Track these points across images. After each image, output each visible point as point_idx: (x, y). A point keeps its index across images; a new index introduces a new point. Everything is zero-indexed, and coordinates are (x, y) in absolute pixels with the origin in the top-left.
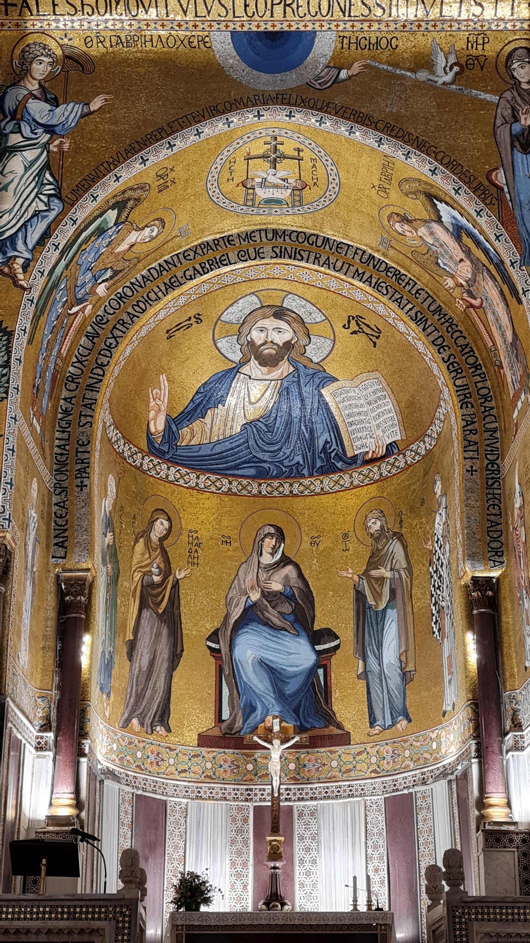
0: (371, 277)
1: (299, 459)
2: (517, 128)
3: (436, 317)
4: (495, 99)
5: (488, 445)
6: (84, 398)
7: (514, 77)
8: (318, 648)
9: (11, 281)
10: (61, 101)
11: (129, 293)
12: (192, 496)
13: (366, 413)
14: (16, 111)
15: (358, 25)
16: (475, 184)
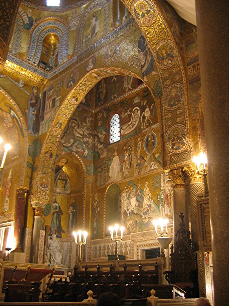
2: (32, 102)
4: (29, 94)
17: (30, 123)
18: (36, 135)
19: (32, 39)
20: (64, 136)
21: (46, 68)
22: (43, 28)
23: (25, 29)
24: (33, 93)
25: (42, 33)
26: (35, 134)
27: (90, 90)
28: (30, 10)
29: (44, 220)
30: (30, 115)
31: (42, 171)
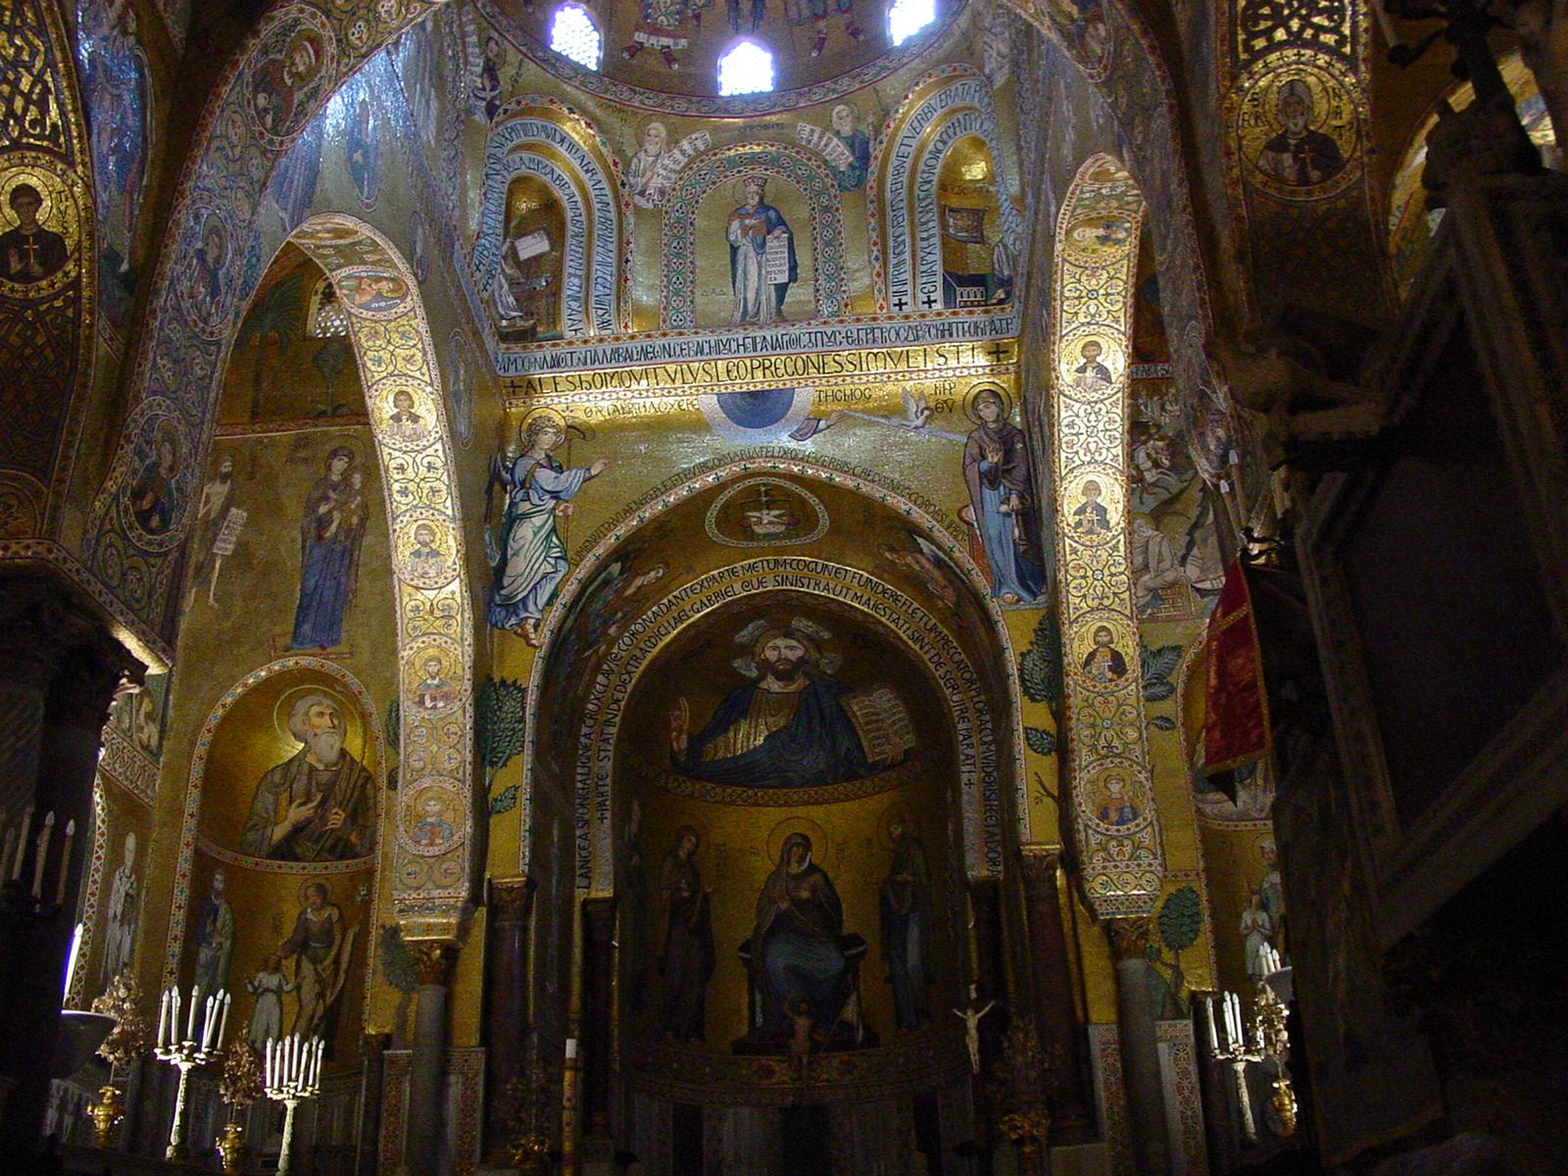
0: (869, 599)
1: (822, 766)
2: (984, 466)
3: (933, 635)
5: (985, 758)
6: (602, 733)
7: (980, 418)
8: (846, 953)
9: (523, 641)
10: (565, 468)
11: (641, 630)
12: (718, 810)
13: (882, 721)
14: (525, 480)
15: (833, 381)
16: (948, 520)
17: (998, 557)
18: (1041, 599)
19: (890, 214)
20: (1190, 545)
21: (987, 295)
22: (914, 143)
23: (846, 194)
24: (984, 424)
25: (921, 167)
26: (1035, 596)
27: (1130, 301)
28: (841, 107)
29: (1175, 968)
30: (993, 523)
31: (1093, 748)
